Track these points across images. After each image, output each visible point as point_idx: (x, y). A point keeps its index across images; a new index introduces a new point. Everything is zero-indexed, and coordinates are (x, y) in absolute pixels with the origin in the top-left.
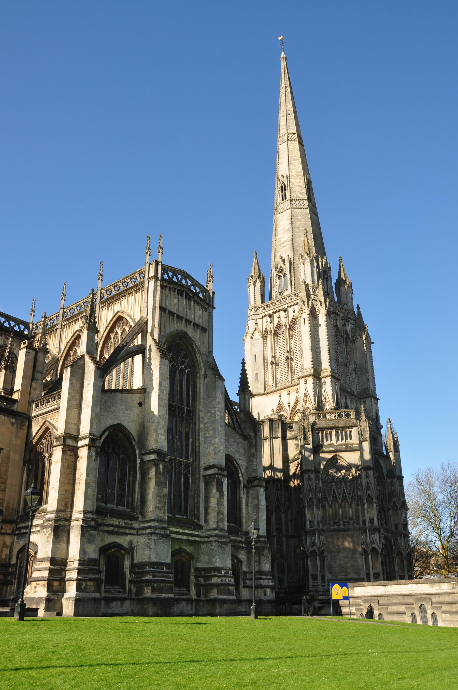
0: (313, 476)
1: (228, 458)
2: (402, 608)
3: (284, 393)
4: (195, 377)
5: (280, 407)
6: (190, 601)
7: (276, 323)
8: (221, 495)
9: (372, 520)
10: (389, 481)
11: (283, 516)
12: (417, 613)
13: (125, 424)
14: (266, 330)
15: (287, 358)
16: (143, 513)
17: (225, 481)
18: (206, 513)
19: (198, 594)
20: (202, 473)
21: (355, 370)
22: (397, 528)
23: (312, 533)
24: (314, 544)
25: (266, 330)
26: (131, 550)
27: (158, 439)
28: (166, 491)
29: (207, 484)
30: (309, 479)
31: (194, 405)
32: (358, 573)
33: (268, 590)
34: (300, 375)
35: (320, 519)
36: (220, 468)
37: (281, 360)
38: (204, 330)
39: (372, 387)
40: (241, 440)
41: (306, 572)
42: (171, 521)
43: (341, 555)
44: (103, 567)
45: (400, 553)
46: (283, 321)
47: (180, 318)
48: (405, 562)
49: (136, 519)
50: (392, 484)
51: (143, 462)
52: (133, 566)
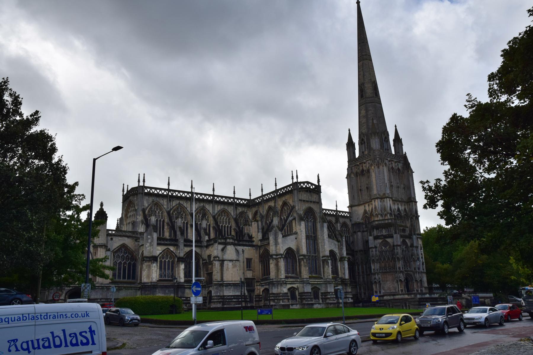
0: (374, 250)
1: (331, 252)
2: (399, 304)
3: (367, 205)
4: (316, 223)
5: (365, 212)
6: (319, 304)
7: (361, 168)
8: (329, 267)
9: (399, 268)
10: (411, 248)
11: (364, 266)
12: (404, 305)
13: (291, 247)
14: (357, 172)
15: (367, 188)
16: (300, 276)
17: (330, 261)
18: (324, 273)
19: (323, 301)
20: (321, 258)
21: (404, 188)
22: (415, 269)
23: (374, 274)
24: (375, 279)
25: (357, 172)
26: (297, 289)
27: (304, 251)
28: (307, 268)
29: (323, 263)
30: (372, 251)
31: (316, 234)
32: (395, 290)
33: (350, 299)
34: (373, 197)
35: (378, 268)
36: (327, 257)
37: (364, 188)
38: (318, 203)
39: (413, 196)
40: (337, 243)
41: (372, 289)
42: (310, 278)
43: (388, 282)
44: (289, 295)
45: (416, 281)
46: (365, 168)
47: (307, 201)
48: (419, 284)
49: (298, 278)
50: (412, 250)
51: (299, 259)
52: (299, 293)
